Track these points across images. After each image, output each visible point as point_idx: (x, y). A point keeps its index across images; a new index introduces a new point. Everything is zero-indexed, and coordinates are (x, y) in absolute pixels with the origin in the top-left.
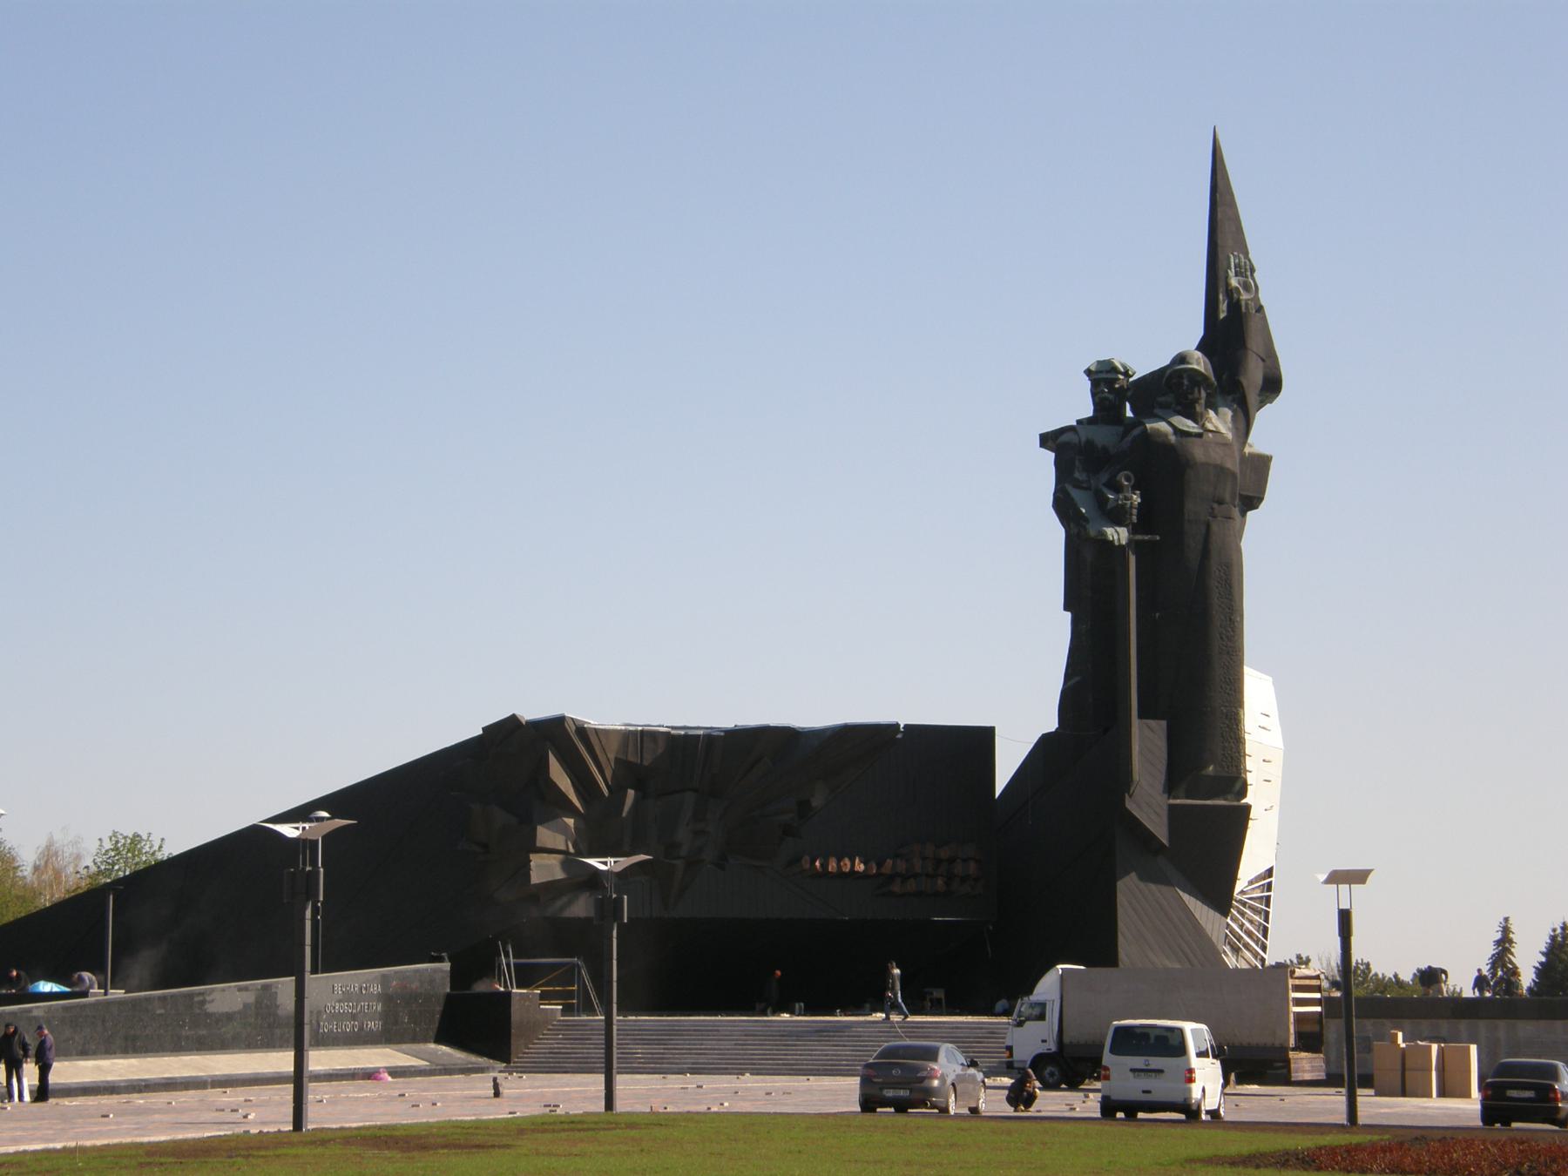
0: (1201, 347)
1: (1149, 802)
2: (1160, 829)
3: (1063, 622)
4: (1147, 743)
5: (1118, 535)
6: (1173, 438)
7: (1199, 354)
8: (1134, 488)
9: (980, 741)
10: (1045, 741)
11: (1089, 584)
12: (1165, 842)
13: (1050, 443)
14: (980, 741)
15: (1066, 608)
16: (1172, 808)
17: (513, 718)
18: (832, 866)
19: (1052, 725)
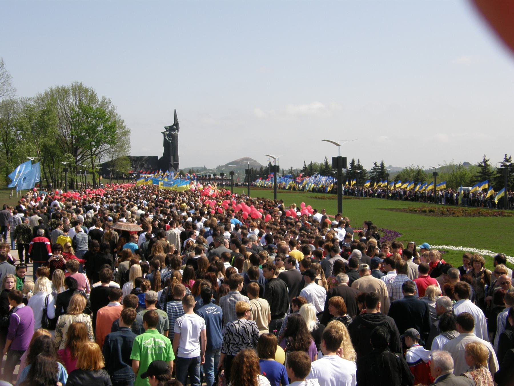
1: (172, 163)
2: (173, 164)
4: (172, 158)
5: (170, 141)
9: (157, 157)
14: (157, 157)
19: (162, 156)
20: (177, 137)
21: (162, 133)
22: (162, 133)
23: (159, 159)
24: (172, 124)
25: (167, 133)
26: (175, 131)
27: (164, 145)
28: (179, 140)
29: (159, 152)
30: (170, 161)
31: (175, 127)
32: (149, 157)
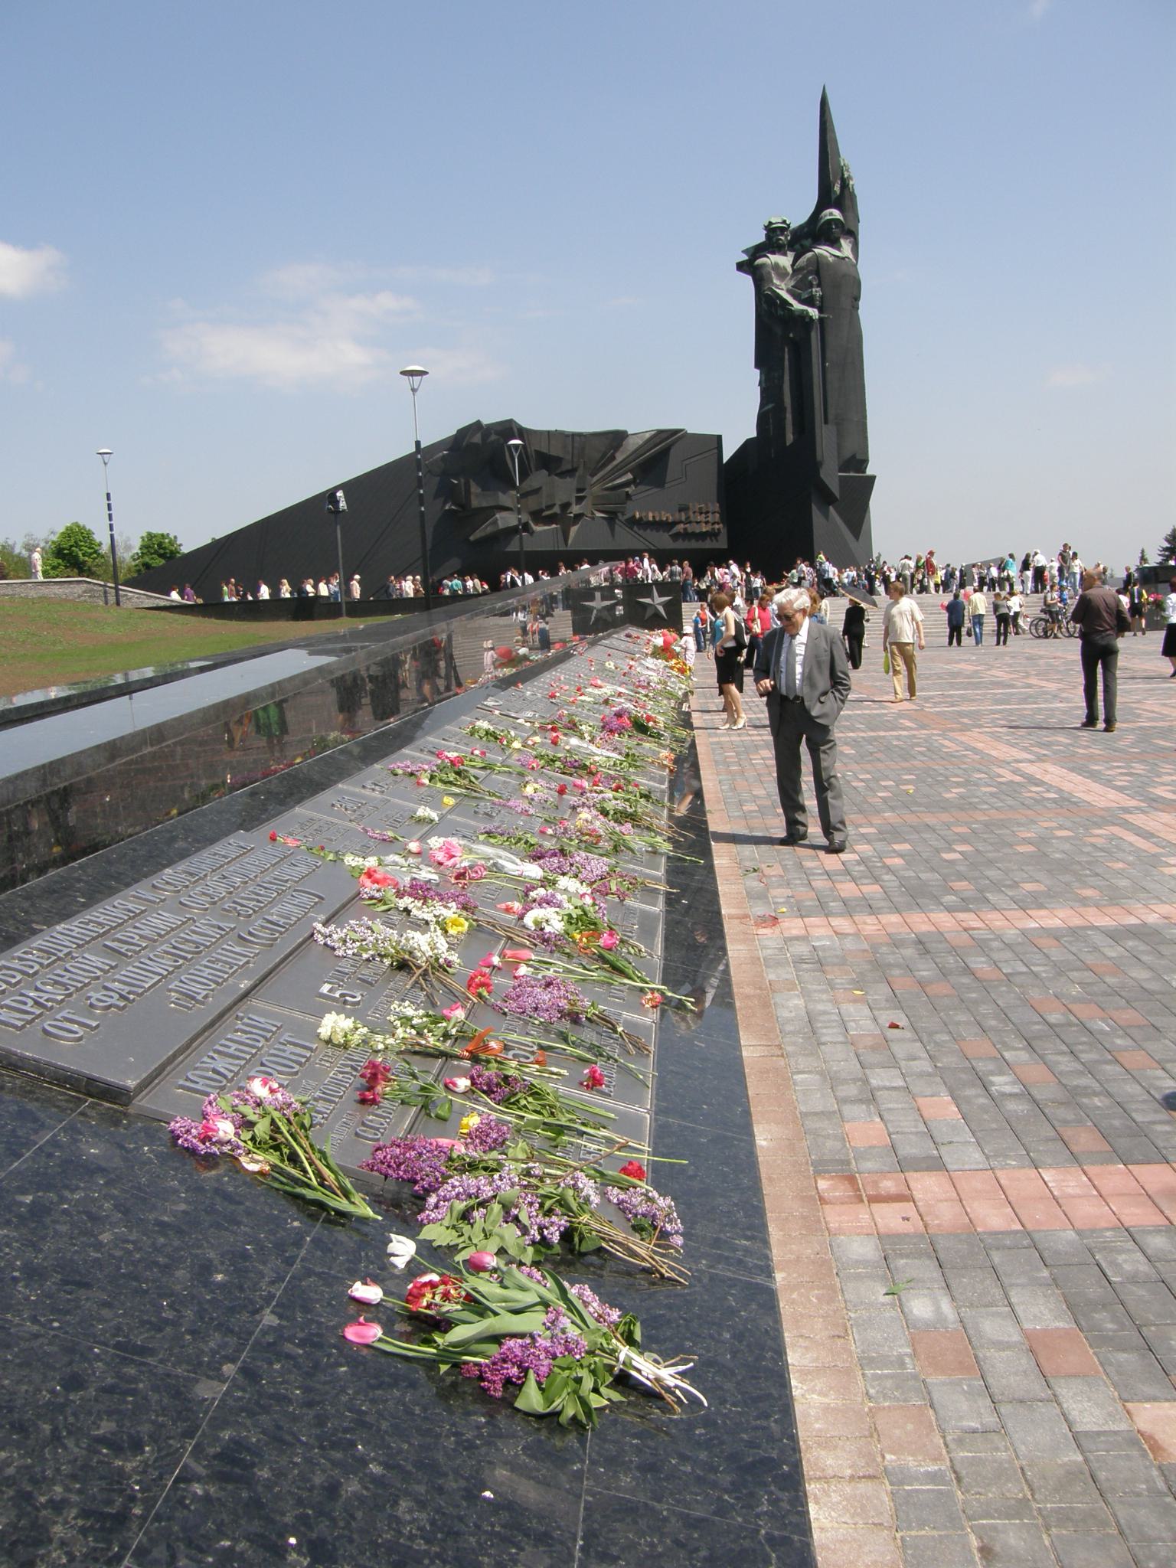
1: (831, 475)
2: (835, 488)
4: (825, 438)
5: (814, 313)
8: (819, 285)
10: (748, 443)
15: (757, 366)
17: (478, 423)
20: (858, 284)
21: (740, 267)
22: (740, 267)
23: (728, 454)
24: (797, 207)
25: (785, 261)
26: (834, 243)
27: (758, 364)
28: (868, 312)
29: (724, 404)
30: (815, 466)
31: (836, 214)
32: (660, 432)
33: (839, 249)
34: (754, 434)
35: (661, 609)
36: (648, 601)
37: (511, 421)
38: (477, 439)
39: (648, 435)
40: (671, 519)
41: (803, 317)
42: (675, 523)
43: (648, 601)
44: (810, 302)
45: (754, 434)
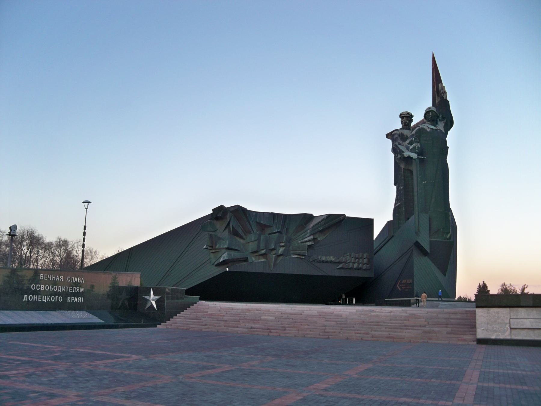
0: (433, 105)
3: (393, 189)
5: (414, 156)
6: (428, 130)
7: (434, 107)
9: (370, 222)
10: (389, 222)
11: (403, 177)
12: (428, 251)
13: (389, 137)
14: (370, 222)
15: (395, 185)
16: (431, 242)
17: (222, 206)
18: (324, 258)
19: (391, 218)
33: (435, 126)
34: (392, 219)
35: (154, 303)
36: (147, 297)
37: (238, 206)
38: (220, 215)
39: (323, 217)
40: (337, 261)
41: (409, 158)
42: (340, 263)
43: (147, 297)
44: (412, 151)
45: (392, 219)
